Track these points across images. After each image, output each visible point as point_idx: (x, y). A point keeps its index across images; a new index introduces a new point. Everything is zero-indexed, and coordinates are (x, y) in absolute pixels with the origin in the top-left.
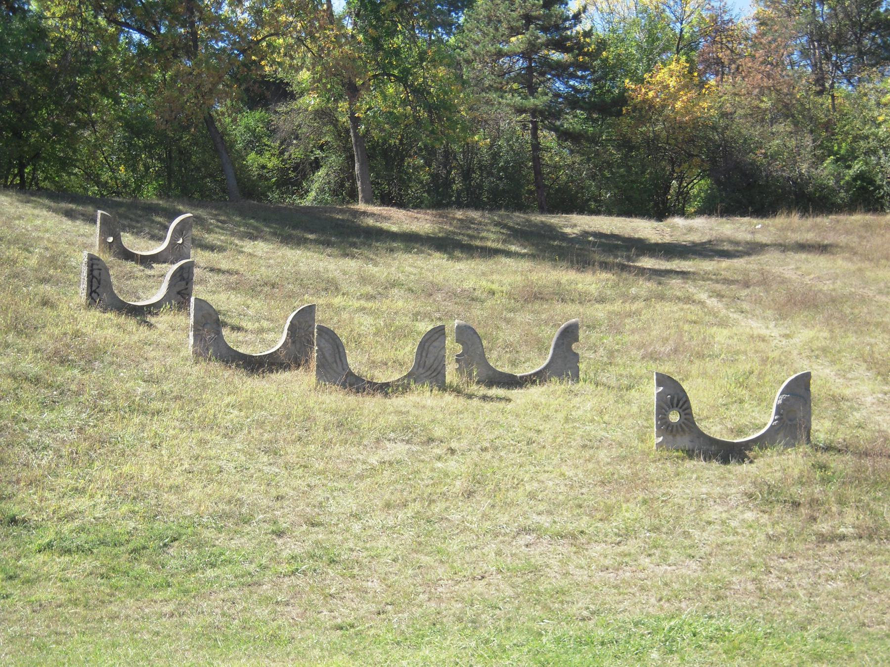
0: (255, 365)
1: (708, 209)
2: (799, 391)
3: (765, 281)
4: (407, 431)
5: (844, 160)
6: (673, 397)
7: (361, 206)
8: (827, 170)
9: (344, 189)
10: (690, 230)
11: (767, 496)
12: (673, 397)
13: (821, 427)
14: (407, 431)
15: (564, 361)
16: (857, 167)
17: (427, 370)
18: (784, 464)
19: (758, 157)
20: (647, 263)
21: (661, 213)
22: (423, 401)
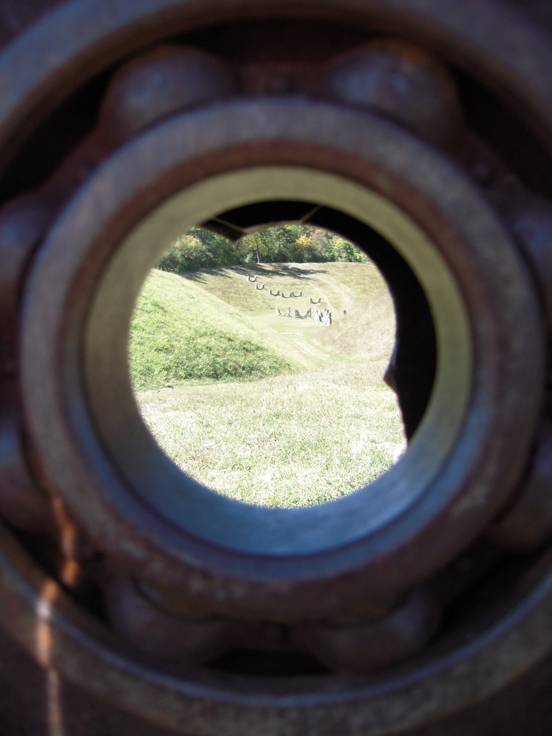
0: (276, 295)
1: (309, 261)
2: (320, 299)
3: (317, 280)
4: (292, 302)
5: (330, 252)
6: (311, 299)
7: (258, 263)
8: (327, 255)
9: (254, 259)
10: (306, 267)
11: (317, 306)
12: (311, 299)
13: (321, 301)
14: (292, 302)
15: (301, 295)
16: (332, 254)
17: (291, 296)
18: (319, 304)
19: (316, 252)
20: (302, 276)
21: (301, 261)
22: (290, 298)
